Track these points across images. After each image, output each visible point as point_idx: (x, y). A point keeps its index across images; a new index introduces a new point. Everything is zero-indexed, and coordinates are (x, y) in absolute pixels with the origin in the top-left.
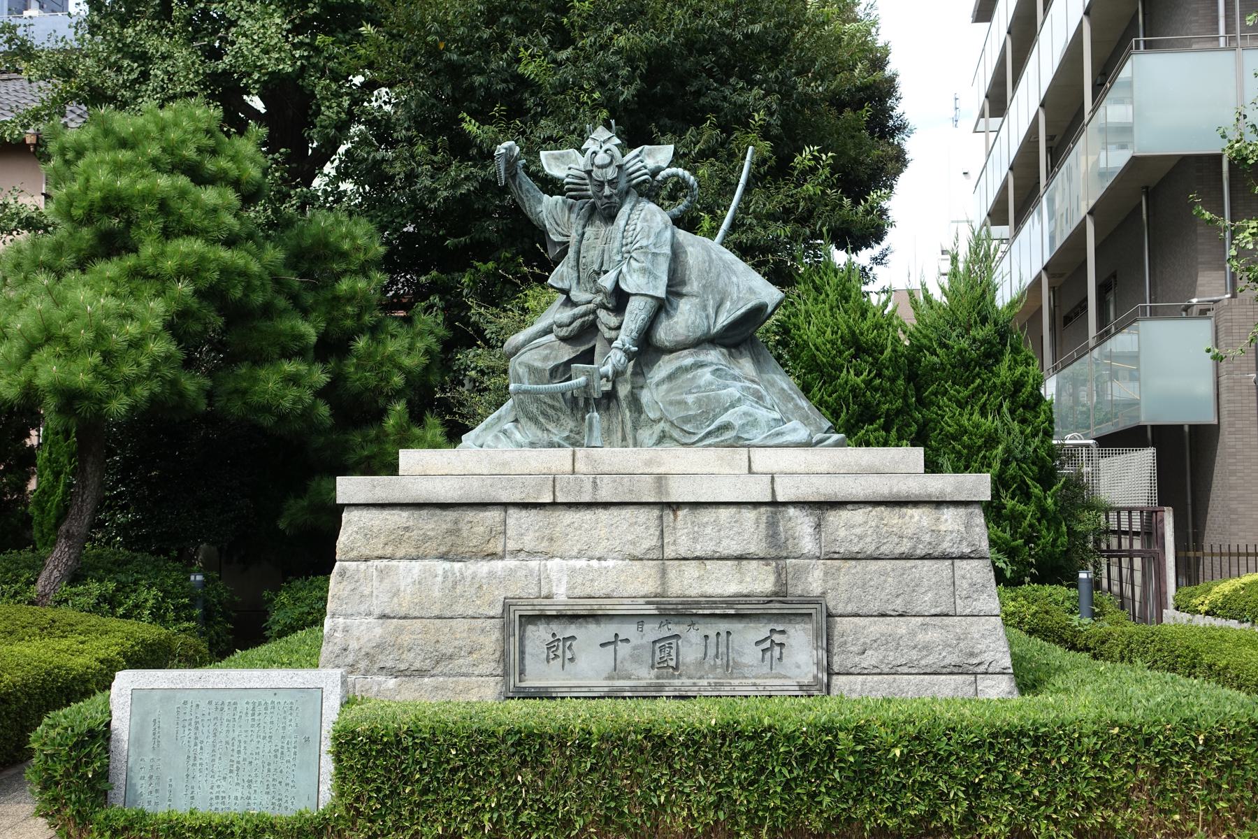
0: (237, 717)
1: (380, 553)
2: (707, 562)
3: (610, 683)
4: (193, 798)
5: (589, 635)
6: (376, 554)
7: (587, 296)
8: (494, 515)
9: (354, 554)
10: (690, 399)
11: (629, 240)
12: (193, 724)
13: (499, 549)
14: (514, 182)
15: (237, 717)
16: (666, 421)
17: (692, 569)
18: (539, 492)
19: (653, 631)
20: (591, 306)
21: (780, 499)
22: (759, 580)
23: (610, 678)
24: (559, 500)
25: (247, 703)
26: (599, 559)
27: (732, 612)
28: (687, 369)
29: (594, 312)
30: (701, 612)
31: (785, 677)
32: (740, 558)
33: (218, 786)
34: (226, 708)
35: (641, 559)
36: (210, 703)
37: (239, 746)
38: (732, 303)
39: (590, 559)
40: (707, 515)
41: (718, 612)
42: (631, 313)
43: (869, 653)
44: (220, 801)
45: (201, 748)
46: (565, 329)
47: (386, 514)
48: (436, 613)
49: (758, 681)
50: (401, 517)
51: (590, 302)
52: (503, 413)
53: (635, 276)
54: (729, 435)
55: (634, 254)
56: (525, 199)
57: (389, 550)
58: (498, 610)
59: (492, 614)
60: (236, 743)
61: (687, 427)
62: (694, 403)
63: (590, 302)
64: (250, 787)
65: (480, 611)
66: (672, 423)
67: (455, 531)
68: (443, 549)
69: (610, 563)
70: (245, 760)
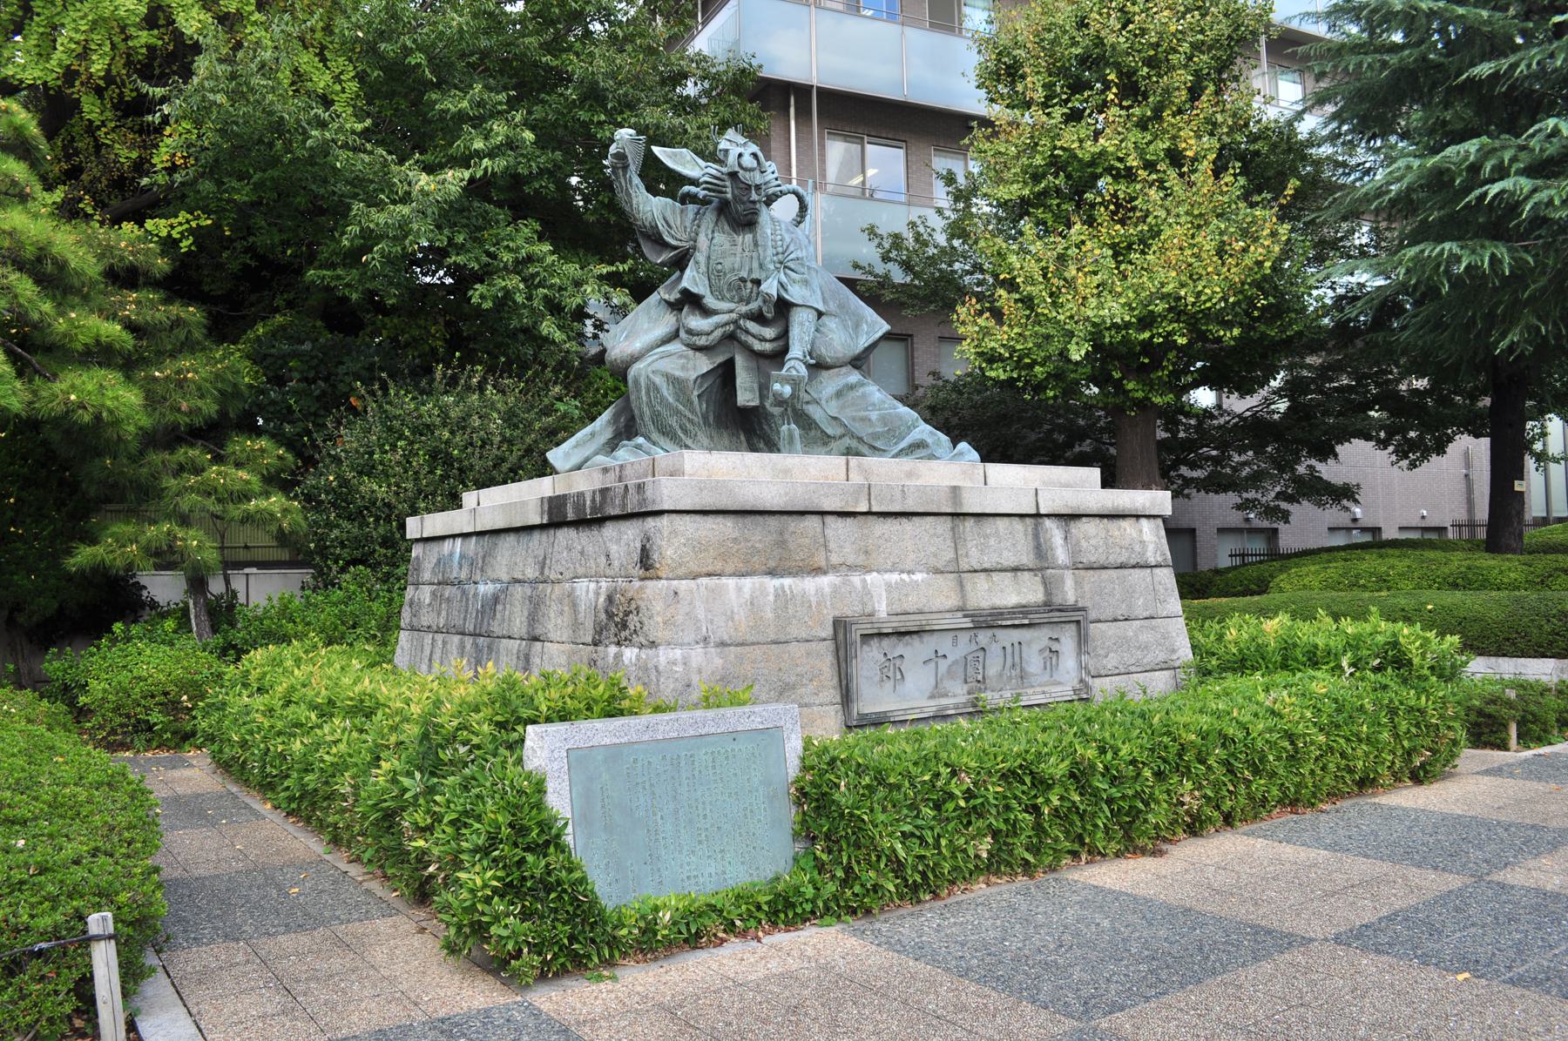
0: (696, 773)
1: (710, 569)
2: (993, 574)
3: (932, 703)
4: (661, 883)
5: (915, 651)
6: (705, 570)
7: (732, 306)
8: (813, 523)
9: (680, 572)
10: (874, 416)
11: (780, 250)
12: (647, 784)
13: (823, 564)
14: (624, 175)
15: (696, 773)
16: (853, 436)
17: (981, 581)
18: (857, 502)
19: (964, 645)
20: (734, 316)
21: (1043, 511)
22: (1027, 592)
23: (932, 697)
24: (874, 509)
25: (706, 753)
26: (909, 572)
27: (1026, 622)
28: (852, 387)
29: (735, 322)
30: (1004, 623)
31: (1059, 683)
32: (1015, 570)
33: (689, 864)
34: (683, 763)
35: (942, 572)
36: (664, 758)
37: (704, 809)
38: (869, 326)
39: (902, 572)
40: (989, 526)
41: (1017, 622)
42: (802, 324)
43: (1112, 655)
44: (693, 881)
45: (662, 818)
46: (704, 338)
47: (710, 522)
48: (773, 637)
49: (1046, 689)
50: (727, 526)
51: (732, 311)
52: (598, 428)
53: (797, 287)
54: (923, 452)
55: (790, 264)
56: (633, 195)
57: (718, 567)
58: (828, 631)
59: (824, 635)
60: (700, 806)
61: (878, 444)
62: (879, 420)
63: (732, 311)
64: (723, 858)
65: (813, 633)
66: (860, 439)
67: (781, 544)
68: (772, 564)
69: (918, 577)
70: (712, 826)
